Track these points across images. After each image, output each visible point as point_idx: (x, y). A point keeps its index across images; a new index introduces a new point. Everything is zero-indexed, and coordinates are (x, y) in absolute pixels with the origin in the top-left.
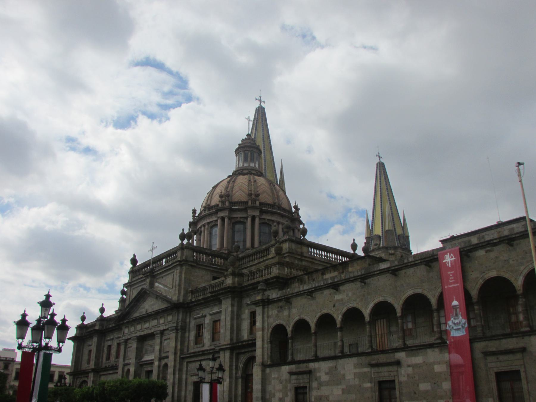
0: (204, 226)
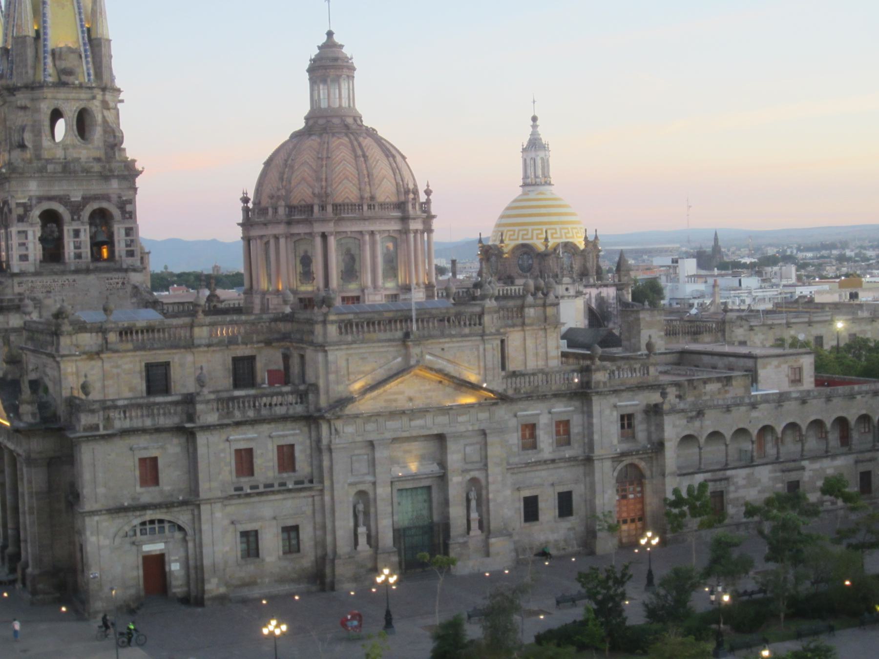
0: (372, 233)
